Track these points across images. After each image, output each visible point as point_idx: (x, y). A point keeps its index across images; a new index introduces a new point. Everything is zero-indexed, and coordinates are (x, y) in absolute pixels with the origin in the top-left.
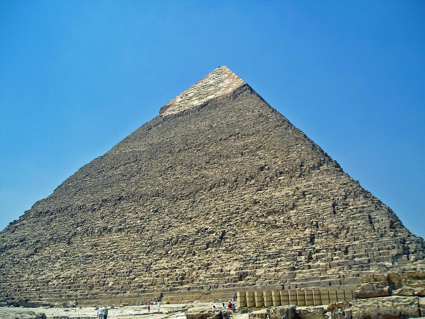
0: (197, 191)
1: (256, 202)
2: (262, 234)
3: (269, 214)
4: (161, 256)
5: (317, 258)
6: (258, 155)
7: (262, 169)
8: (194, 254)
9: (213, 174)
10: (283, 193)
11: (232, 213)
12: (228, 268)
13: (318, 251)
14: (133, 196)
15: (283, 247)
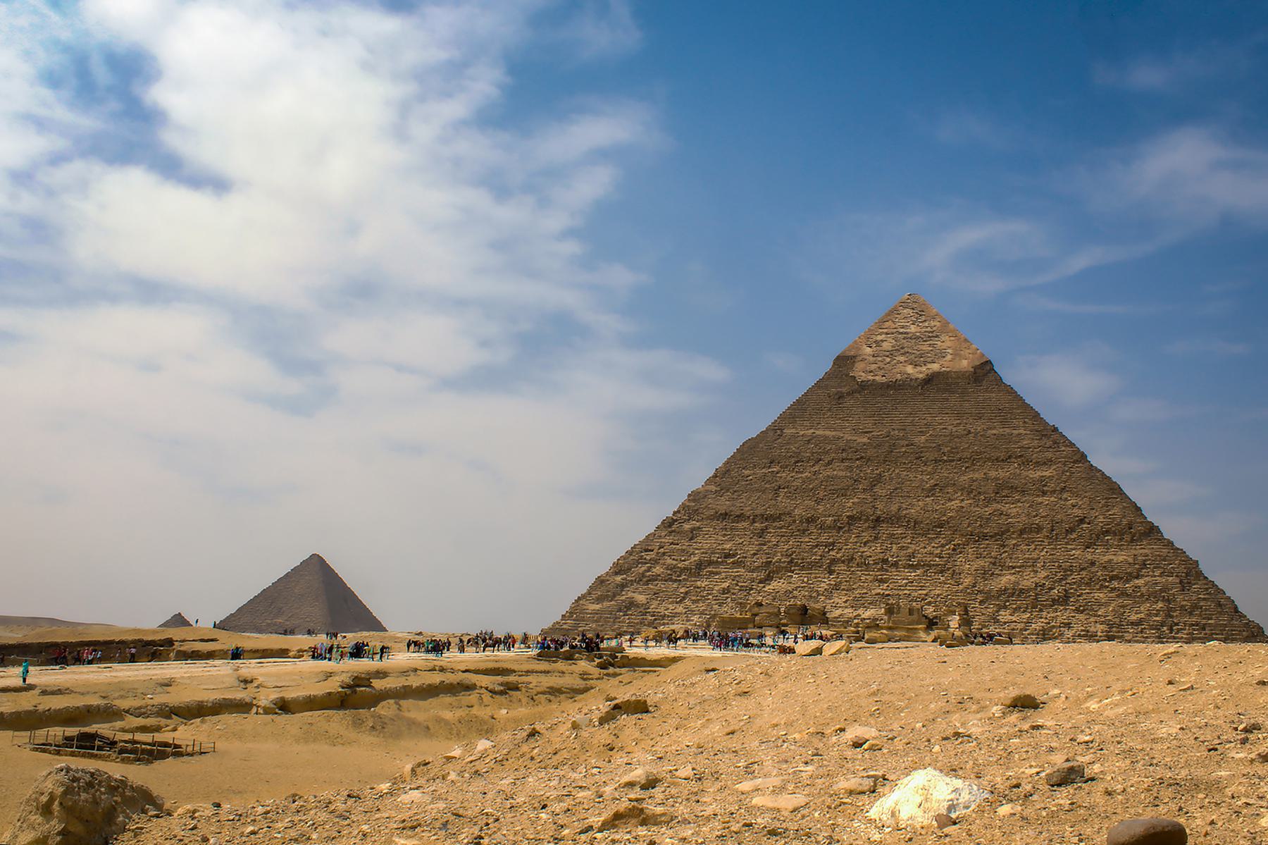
0: (1003, 533)
1: (1093, 564)
2: (1111, 600)
3: (1112, 578)
4: (1000, 608)
5: (1178, 631)
6: (1066, 499)
7: (1082, 521)
8: (1041, 610)
9: (1016, 511)
10: (1121, 558)
11: (1066, 570)
12: (1092, 629)
13: (1177, 624)
14: (899, 519)
15: (1142, 616)
